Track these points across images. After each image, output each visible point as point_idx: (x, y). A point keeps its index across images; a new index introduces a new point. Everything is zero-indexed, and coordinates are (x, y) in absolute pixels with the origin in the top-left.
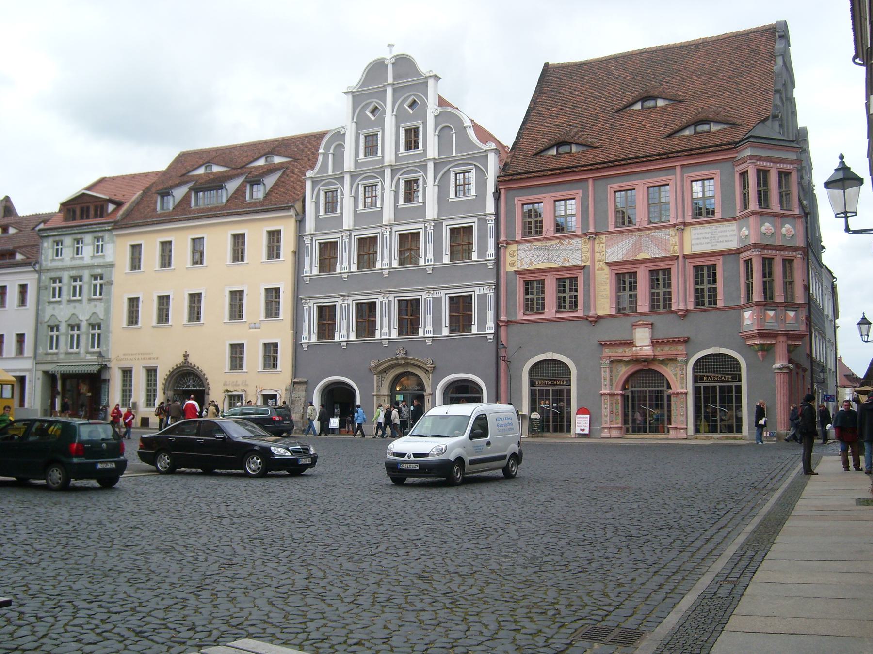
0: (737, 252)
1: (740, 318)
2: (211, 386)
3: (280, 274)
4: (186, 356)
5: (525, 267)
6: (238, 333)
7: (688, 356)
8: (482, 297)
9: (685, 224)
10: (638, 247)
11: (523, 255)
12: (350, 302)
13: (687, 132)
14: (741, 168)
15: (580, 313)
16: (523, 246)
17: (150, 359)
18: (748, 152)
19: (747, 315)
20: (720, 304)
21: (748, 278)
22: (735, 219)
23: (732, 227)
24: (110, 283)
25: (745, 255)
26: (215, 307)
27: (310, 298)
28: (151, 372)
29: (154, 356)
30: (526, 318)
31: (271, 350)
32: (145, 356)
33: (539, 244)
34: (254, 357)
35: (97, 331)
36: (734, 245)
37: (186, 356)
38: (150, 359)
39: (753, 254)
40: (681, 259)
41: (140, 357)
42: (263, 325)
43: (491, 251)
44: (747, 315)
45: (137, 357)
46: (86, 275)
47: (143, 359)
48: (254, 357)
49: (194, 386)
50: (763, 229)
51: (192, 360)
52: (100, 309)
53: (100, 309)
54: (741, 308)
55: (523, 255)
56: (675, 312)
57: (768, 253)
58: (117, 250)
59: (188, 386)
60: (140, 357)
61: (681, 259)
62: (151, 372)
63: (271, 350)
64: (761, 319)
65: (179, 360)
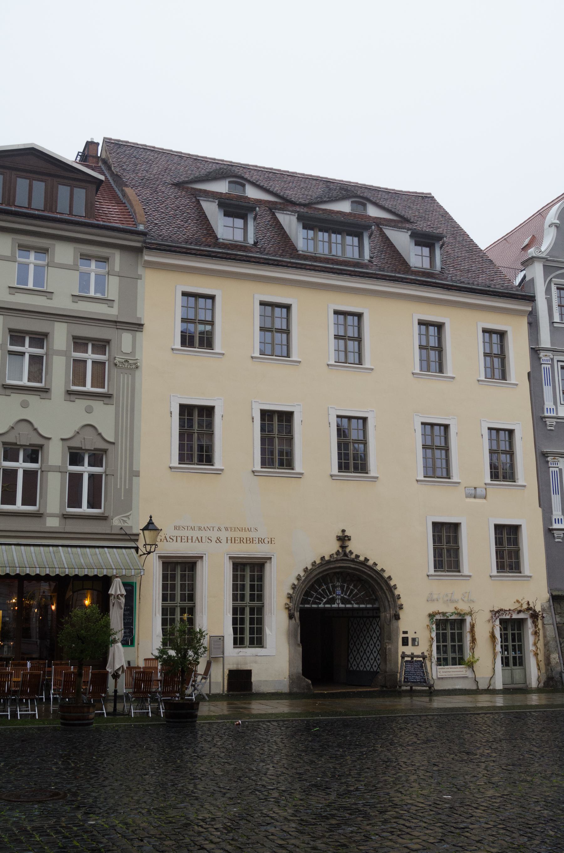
2: (402, 601)
3: (511, 406)
4: (343, 539)
6: (446, 504)
17: (252, 541)
24: (131, 366)
26: (394, 450)
28: (249, 574)
29: (261, 534)
31: (507, 538)
32: (238, 534)
34: (478, 549)
35: (86, 469)
37: (343, 539)
38: (252, 541)
41: (223, 535)
42: (490, 490)
45: (214, 535)
46: (60, 336)
47: (233, 540)
48: (478, 549)
49: (344, 601)
51: (357, 547)
52: (103, 417)
53: (103, 417)
58: (160, 295)
59: (332, 601)
60: (223, 535)
62: (249, 574)
63: (507, 538)
65: (330, 548)
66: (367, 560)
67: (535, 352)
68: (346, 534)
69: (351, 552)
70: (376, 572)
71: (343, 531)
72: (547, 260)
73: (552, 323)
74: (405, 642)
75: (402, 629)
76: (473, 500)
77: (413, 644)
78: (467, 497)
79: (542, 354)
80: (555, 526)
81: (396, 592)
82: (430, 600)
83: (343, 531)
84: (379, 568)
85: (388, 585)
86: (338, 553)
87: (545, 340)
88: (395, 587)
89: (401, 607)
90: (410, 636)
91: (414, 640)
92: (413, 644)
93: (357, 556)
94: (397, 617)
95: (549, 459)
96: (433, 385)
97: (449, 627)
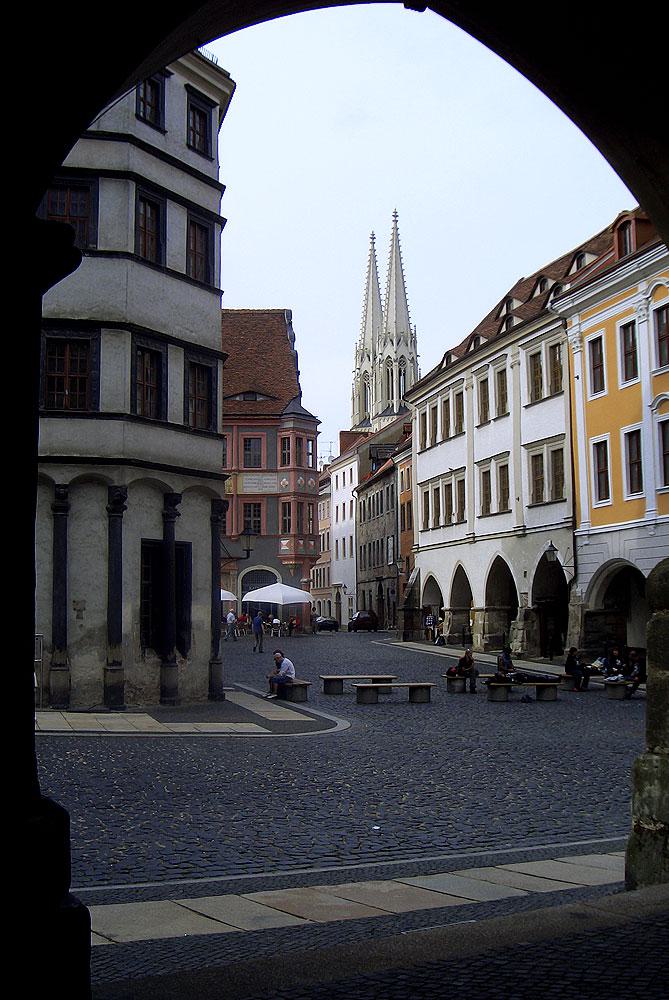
0: (278, 496)
1: (278, 545)
9: (240, 471)
13: (238, 399)
14: (284, 434)
18: (291, 425)
19: (284, 542)
20: (263, 533)
22: (277, 471)
23: (275, 476)
25: (284, 499)
36: (275, 490)
39: (291, 499)
40: (235, 498)
44: (284, 542)
54: (279, 538)
56: (230, 537)
57: (302, 499)
61: (235, 498)
64: (297, 545)
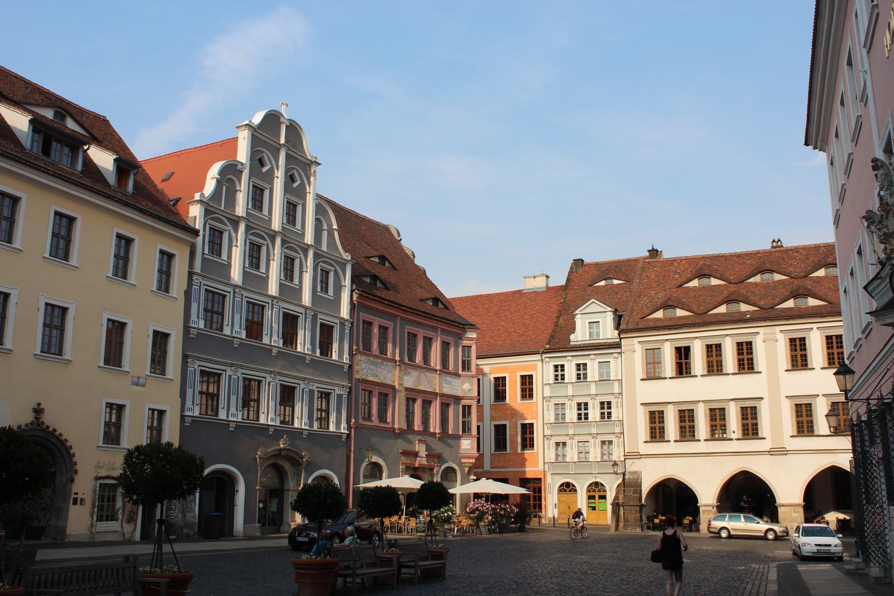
2: (78, 467)
5: (364, 377)
7: (440, 467)
8: (340, 397)
10: (419, 380)
11: (363, 366)
12: (239, 375)
15: (390, 426)
16: (363, 358)
21: (464, 416)
25: (464, 402)
26: (84, 339)
27: (199, 359)
30: (363, 423)
33: (372, 359)
37: (38, 411)
43: (346, 356)
50: (464, 387)
51: (49, 419)
55: (363, 366)
66: (55, 430)
67: (191, 274)
68: (41, 407)
69: (43, 423)
70: (61, 441)
71: (39, 404)
72: (209, 205)
73: (203, 254)
74: (75, 503)
75: (74, 491)
76: (135, 387)
77: (81, 504)
78: (133, 384)
79: (195, 277)
80: (187, 413)
81: (74, 460)
82: (98, 467)
83: (39, 404)
84: (63, 438)
85: (68, 452)
86: (32, 423)
87: (198, 268)
88: (74, 455)
89: (76, 472)
90: (79, 496)
91: (82, 500)
92: (81, 504)
93: (48, 427)
94: (72, 480)
95: (189, 360)
96: (118, 289)
97: (107, 490)
